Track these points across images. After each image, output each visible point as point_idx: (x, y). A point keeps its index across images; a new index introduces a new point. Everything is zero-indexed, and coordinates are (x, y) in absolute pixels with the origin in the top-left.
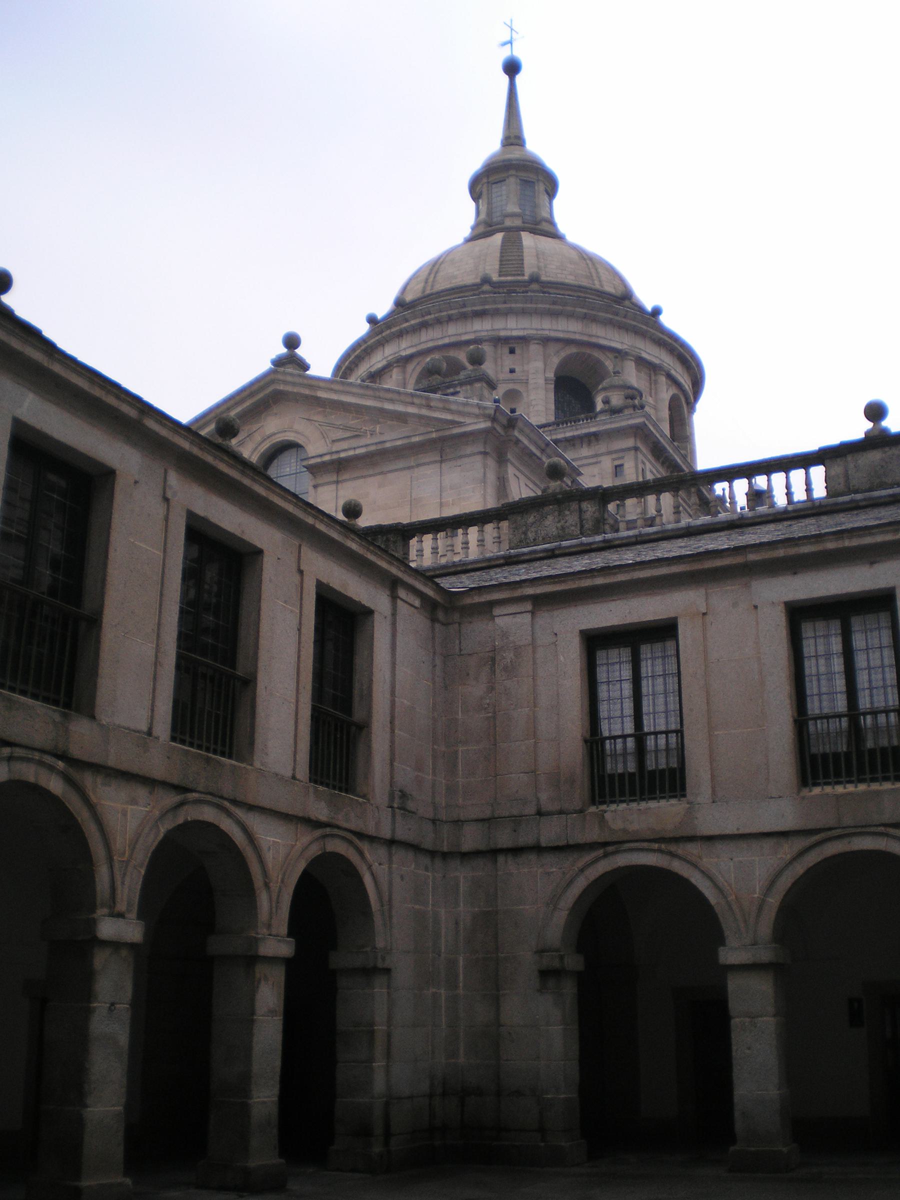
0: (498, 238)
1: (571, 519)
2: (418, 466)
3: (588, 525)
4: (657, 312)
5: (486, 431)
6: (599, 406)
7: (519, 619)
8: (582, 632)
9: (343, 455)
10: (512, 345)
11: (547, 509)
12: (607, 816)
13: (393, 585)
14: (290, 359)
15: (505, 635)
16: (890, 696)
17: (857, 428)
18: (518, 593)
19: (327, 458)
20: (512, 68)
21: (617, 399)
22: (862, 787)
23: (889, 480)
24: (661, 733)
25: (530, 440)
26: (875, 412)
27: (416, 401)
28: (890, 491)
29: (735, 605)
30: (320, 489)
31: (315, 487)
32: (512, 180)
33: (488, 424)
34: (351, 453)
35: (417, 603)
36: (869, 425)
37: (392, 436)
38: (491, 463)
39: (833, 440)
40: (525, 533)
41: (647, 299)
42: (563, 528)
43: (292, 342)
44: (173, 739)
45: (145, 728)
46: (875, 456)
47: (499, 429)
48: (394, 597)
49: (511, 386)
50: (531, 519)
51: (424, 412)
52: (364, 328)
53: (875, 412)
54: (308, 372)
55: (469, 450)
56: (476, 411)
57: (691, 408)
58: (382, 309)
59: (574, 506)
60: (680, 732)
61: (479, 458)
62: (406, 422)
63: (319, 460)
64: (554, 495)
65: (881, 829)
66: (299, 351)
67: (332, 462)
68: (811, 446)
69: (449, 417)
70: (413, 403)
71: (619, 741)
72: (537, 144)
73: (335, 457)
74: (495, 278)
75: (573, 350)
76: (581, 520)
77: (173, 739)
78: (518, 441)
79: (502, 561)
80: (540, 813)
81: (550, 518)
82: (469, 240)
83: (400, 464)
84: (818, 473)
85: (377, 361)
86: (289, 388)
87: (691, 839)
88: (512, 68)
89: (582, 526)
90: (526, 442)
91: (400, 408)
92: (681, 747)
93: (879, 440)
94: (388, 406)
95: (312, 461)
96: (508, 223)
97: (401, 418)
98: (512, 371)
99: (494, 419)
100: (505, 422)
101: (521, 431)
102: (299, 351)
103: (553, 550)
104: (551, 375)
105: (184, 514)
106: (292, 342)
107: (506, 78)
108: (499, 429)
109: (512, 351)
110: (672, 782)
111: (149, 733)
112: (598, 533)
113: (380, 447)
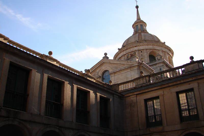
0: (138, 34)
1: (145, 80)
2: (127, 72)
3: (147, 81)
4: (164, 43)
5: (137, 65)
6: (156, 59)
7: (134, 98)
8: (144, 99)
9: (115, 71)
10: (141, 51)
11: (140, 79)
12: (150, 129)
13: (113, 94)
14: (106, 57)
15: (132, 101)
16: (195, 106)
17: (189, 61)
18: (134, 94)
19: (112, 72)
20: (137, 7)
21: (159, 58)
22: (191, 121)
23: (195, 69)
24: (158, 115)
25: (145, 66)
26: (192, 58)
27: (126, 62)
28: (194, 71)
29: (168, 93)
30: (112, 77)
31: (111, 77)
32: (139, 25)
33: (138, 64)
34: (116, 71)
35: (118, 97)
36: (191, 60)
37: (122, 67)
38: (139, 70)
39: (185, 63)
40: (138, 83)
41: (162, 41)
42: (143, 82)
43: (106, 54)
44: (76, 122)
45: (71, 121)
46: (192, 65)
47: (140, 65)
48: (113, 96)
49: (142, 58)
50: (138, 81)
51: (127, 63)
53: (192, 58)
55: (135, 68)
56: (136, 62)
57: (172, 58)
58: (120, 47)
59: (145, 78)
60: (161, 114)
61: (137, 70)
62: (124, 65)
63: (111, 73)
64: (142, 77)
65: (195, 128)
67: (113, 73)
68: (181, 65)
69: (131, 64)
70: (125, 62)
71: (152, 117)
72: (142, 18)
73: (114, 72)
74: (138, 40)
75: (151, 50)
76: (146, 80)
77: (76, 122)
78: (143, 67)
79: (134, 88)
80: (140, 130)
81: (141, 80)
83: (124, 72)
84: (183, 69)
85: (120, 55)
86: (106, 62)
87: (164, 132)
88: (137, 7)
89: (146, 81)
90: (144, 67)
91: (123, 63)
92: (161, 117)
93: (192, 62)
94: (121, 63)
95: (110, 73)
96: (139, 31)
97: (124, 64)
98: (142, 55)
99: (138, 63)
100: (140, 64)
101: (143, 65)
103: (142, 86)
104: (148, 55)
105: (76, 87)
106: (106, 54)
107: (136, 9)
108: (140, 65)
109: (141, 52)
110: (160, 123)
111: (72, 121)
112: (149, 82)
113: (121, 70)
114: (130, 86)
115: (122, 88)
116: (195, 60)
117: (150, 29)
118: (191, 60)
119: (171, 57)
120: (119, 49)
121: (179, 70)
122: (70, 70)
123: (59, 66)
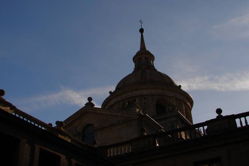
4: (180, 86)
9: (103, 126)
17: (214, 116)
20: (142, 31)
26: (219, 111)
36: (218, 115)
43: (90, 99)
52: (109, 95)
53: (219, 111)
54: (94, 107)
57: (190, 110)
66: (92, 102)
68: (204, 121)
72: (148, 49)
82: (133, 72)
84: (206, 127)
85: (112, 102)
88: (142, 31)
102: (92, 102)
107: (141, 34)
109: (145, 99)
114: (126, 150)
115: (111, 153)
116: (224, 114)
117: (160, 66)
118: (218, 115)
119: (189, 107)
120: (110, 92)
121: (200, 128)
122: (31, 121)
123: (14, 114)
